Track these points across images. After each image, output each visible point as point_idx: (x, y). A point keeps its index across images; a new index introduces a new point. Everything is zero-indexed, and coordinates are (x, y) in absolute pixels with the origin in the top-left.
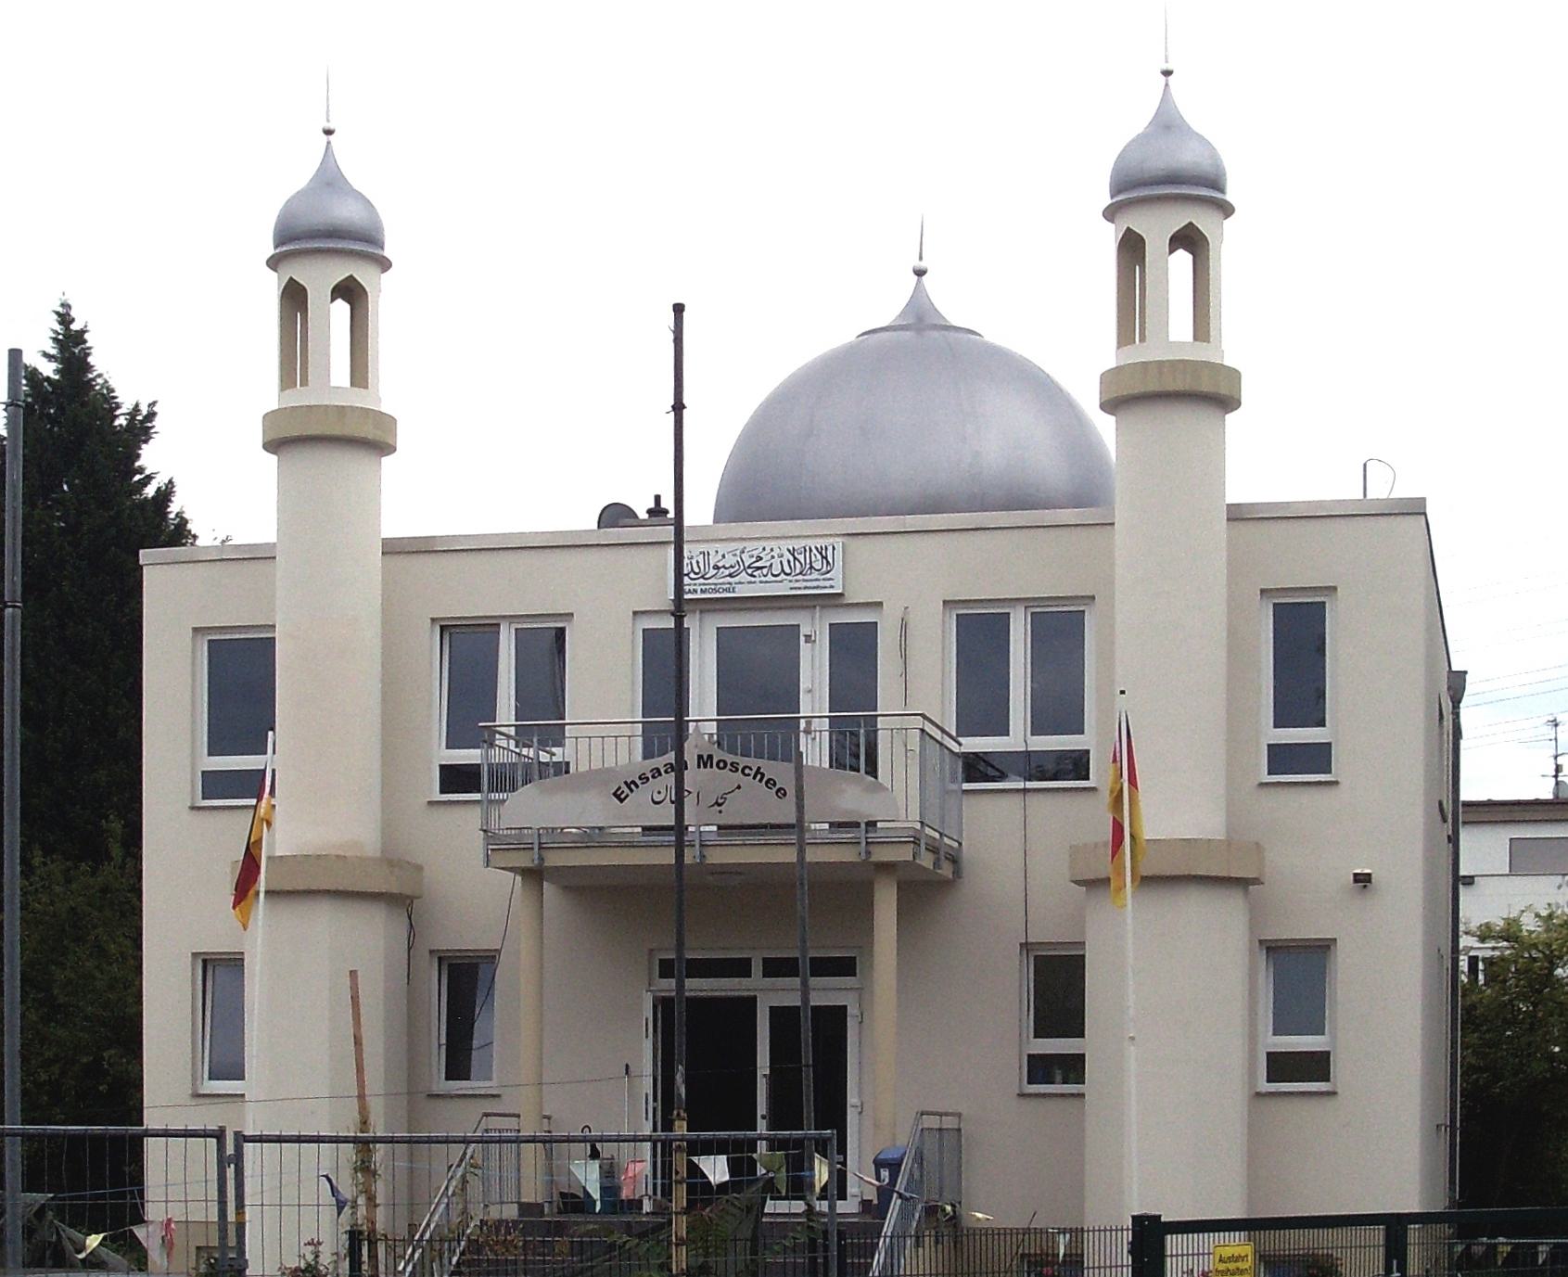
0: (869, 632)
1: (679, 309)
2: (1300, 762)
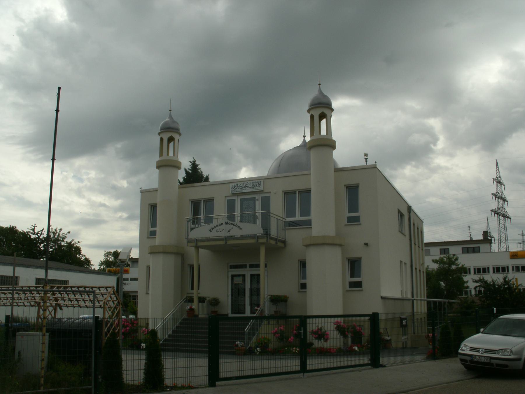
0: (268, 198)
1: (59, 88)
2: (354, 220)
